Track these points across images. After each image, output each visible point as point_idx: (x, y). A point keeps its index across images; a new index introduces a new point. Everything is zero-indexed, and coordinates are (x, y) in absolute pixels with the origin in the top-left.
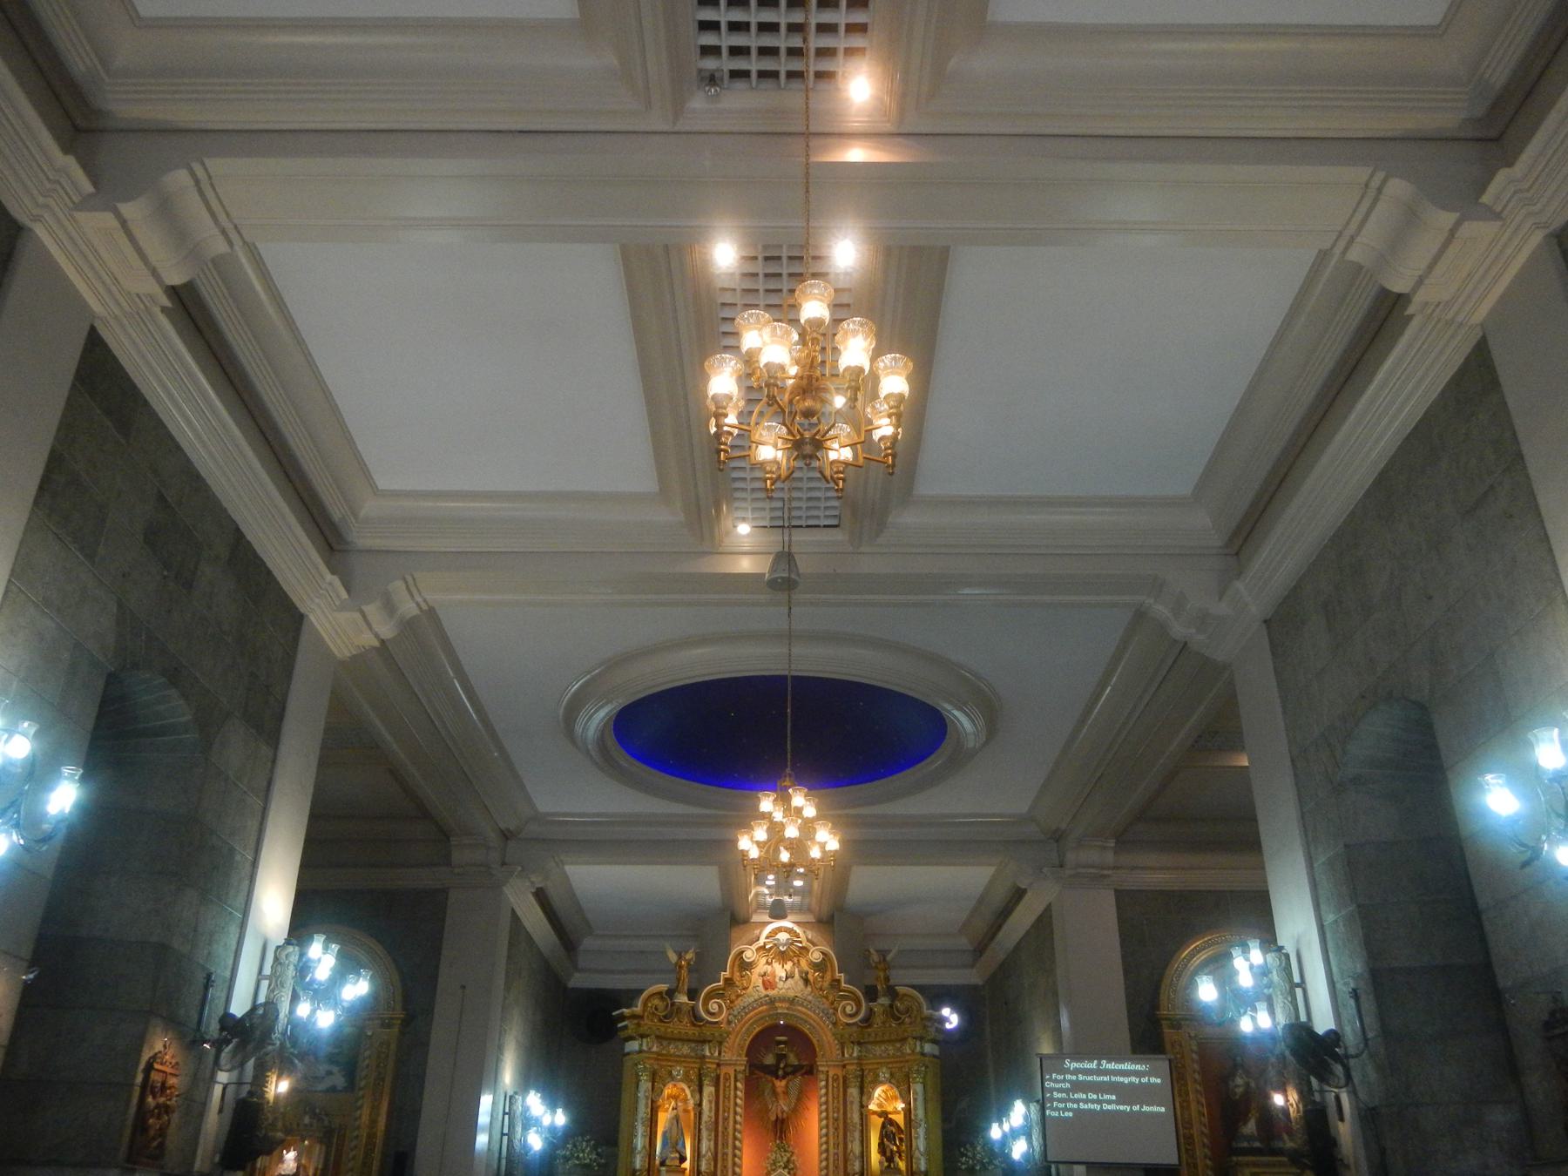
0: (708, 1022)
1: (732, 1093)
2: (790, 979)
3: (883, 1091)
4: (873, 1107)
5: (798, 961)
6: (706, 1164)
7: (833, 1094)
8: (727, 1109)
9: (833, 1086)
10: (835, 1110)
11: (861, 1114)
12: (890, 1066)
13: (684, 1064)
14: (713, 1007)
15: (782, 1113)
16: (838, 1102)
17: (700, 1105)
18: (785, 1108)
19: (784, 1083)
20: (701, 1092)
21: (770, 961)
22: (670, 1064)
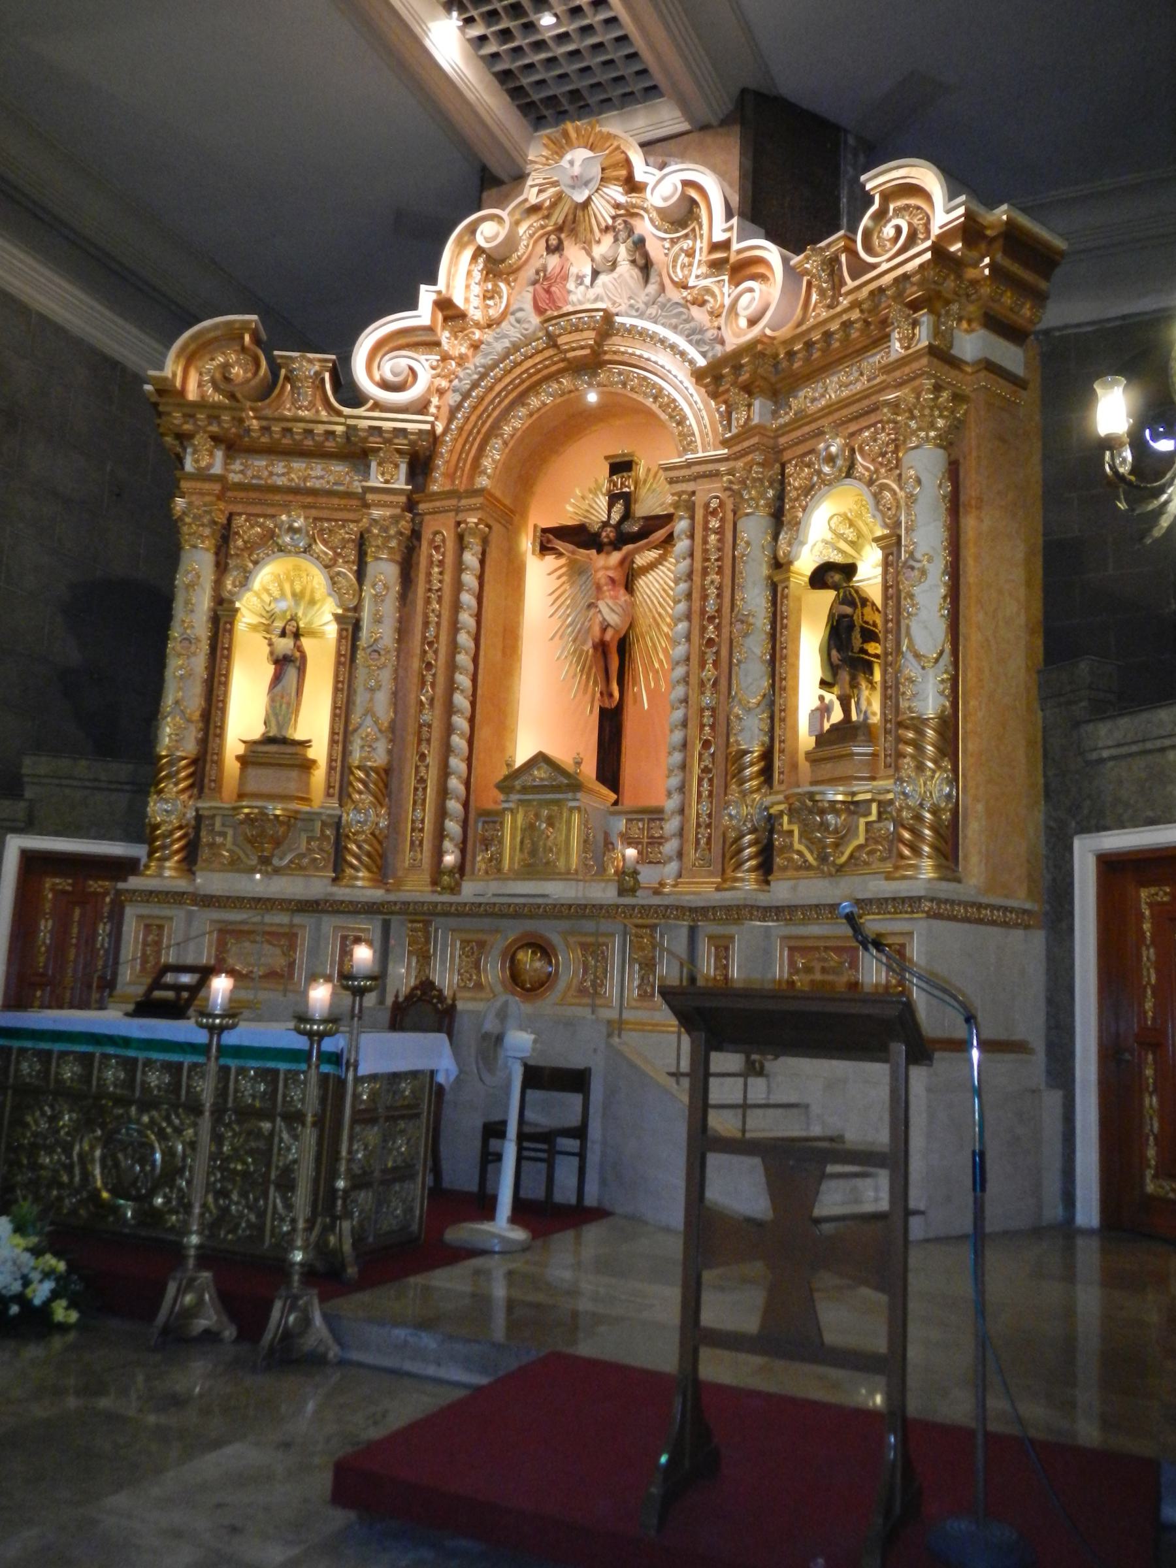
0: (377, 406)
1: (447, 578)
2: (603, 278)
3: (845, 517)
4: (805, 563)
5: (625, 222)
6: (362, 747)
7: (705, 551)
8: (433, 618)
9: (706, 528)
10: (712, 591)
11: (774, 587)
12: (853, 427)
13: (314, 513)
14: (392, 365)
15: (604, 630)
16: (720, 571)
17: (357, 609)
18: (613, 619)
19: (616, 557)
20: (360, 575)
21: (553, 240)
22: (270, 511)
